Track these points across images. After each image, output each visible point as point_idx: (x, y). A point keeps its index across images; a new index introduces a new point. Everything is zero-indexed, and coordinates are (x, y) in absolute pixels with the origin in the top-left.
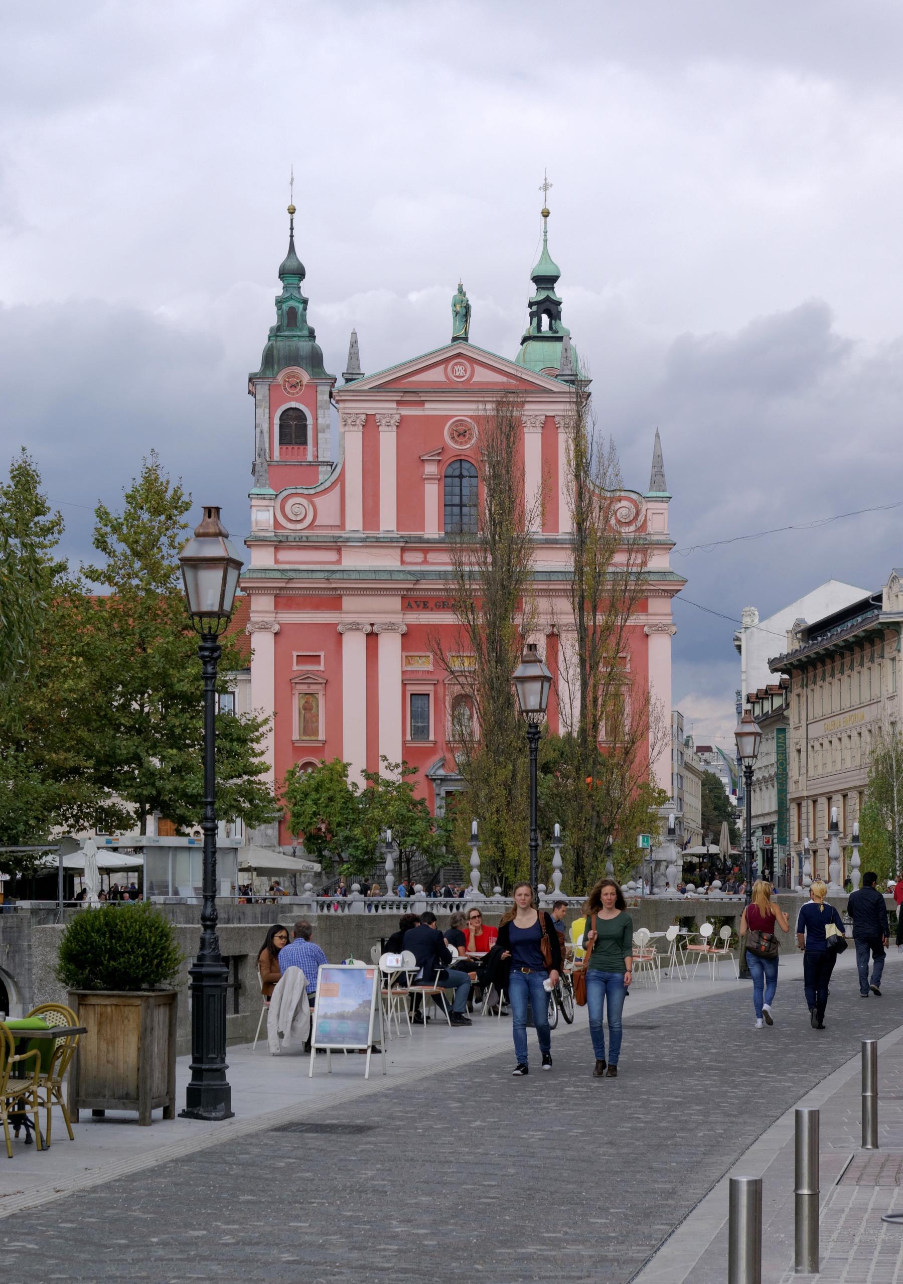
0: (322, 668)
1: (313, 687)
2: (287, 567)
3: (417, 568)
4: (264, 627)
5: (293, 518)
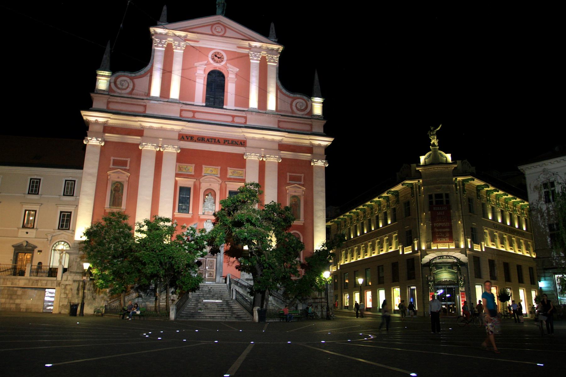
0: (128, 168)
3: (189, 120)
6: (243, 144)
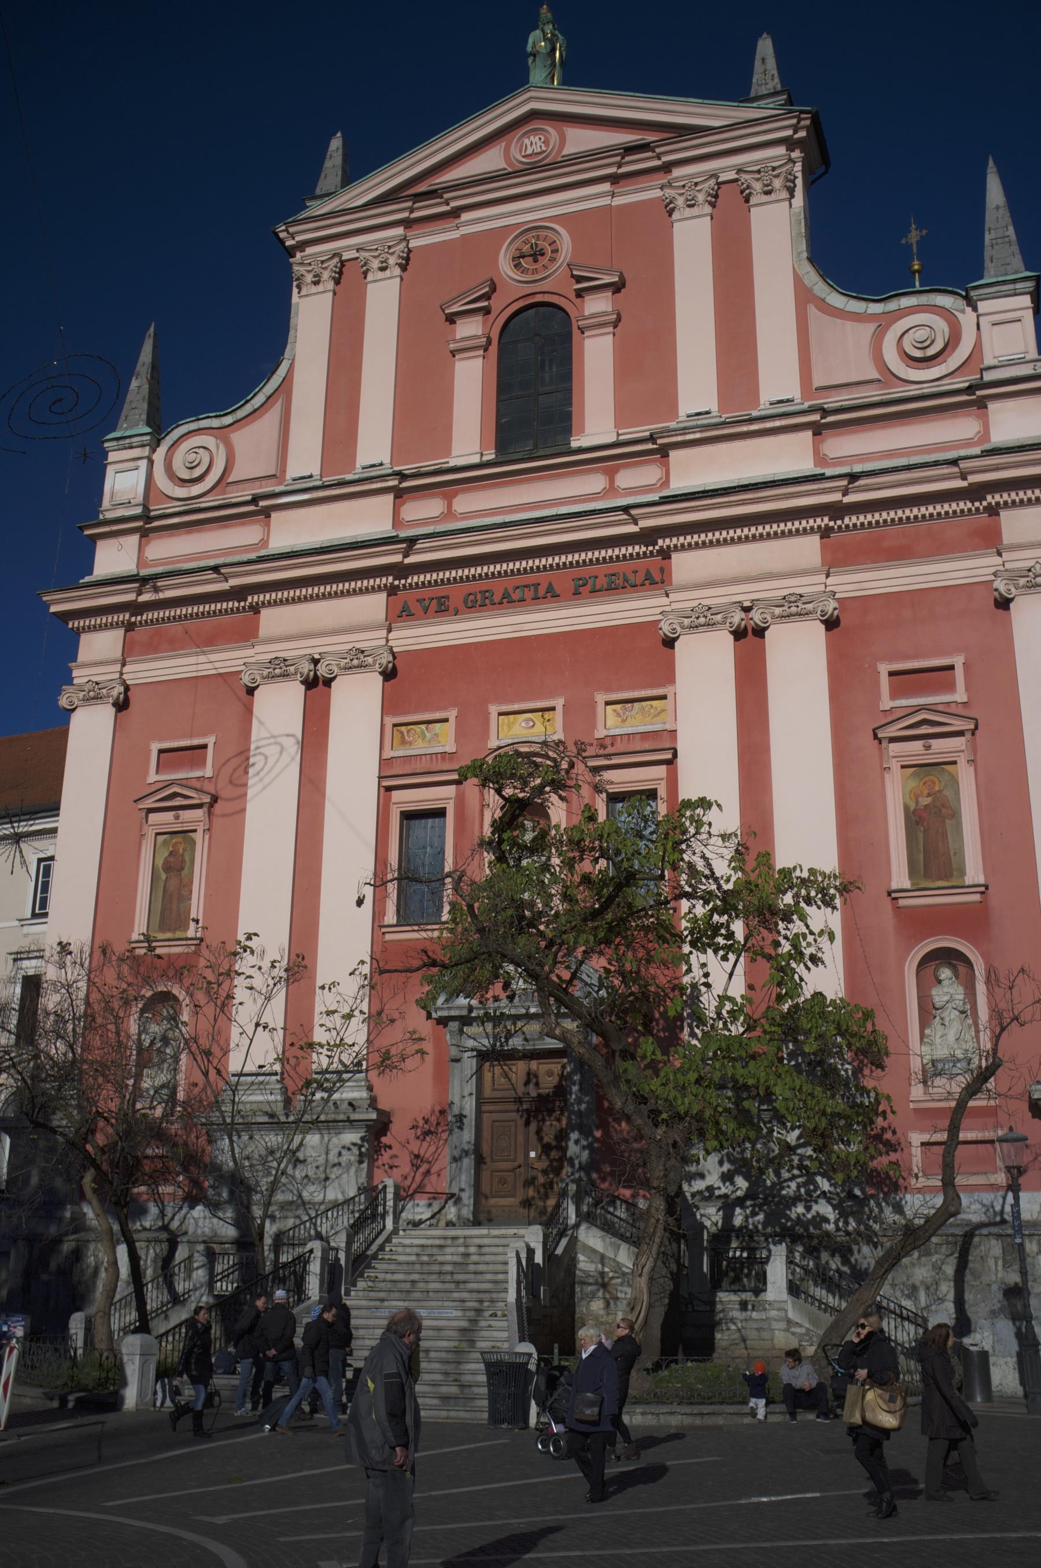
0: (208, 772)
1: (187, 815)
2: (160, 569)
4: (93, 695)
5: (185, 475)
6: (657, 577)
